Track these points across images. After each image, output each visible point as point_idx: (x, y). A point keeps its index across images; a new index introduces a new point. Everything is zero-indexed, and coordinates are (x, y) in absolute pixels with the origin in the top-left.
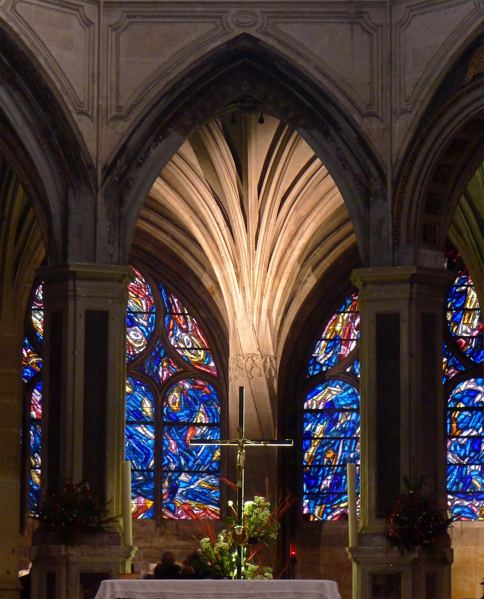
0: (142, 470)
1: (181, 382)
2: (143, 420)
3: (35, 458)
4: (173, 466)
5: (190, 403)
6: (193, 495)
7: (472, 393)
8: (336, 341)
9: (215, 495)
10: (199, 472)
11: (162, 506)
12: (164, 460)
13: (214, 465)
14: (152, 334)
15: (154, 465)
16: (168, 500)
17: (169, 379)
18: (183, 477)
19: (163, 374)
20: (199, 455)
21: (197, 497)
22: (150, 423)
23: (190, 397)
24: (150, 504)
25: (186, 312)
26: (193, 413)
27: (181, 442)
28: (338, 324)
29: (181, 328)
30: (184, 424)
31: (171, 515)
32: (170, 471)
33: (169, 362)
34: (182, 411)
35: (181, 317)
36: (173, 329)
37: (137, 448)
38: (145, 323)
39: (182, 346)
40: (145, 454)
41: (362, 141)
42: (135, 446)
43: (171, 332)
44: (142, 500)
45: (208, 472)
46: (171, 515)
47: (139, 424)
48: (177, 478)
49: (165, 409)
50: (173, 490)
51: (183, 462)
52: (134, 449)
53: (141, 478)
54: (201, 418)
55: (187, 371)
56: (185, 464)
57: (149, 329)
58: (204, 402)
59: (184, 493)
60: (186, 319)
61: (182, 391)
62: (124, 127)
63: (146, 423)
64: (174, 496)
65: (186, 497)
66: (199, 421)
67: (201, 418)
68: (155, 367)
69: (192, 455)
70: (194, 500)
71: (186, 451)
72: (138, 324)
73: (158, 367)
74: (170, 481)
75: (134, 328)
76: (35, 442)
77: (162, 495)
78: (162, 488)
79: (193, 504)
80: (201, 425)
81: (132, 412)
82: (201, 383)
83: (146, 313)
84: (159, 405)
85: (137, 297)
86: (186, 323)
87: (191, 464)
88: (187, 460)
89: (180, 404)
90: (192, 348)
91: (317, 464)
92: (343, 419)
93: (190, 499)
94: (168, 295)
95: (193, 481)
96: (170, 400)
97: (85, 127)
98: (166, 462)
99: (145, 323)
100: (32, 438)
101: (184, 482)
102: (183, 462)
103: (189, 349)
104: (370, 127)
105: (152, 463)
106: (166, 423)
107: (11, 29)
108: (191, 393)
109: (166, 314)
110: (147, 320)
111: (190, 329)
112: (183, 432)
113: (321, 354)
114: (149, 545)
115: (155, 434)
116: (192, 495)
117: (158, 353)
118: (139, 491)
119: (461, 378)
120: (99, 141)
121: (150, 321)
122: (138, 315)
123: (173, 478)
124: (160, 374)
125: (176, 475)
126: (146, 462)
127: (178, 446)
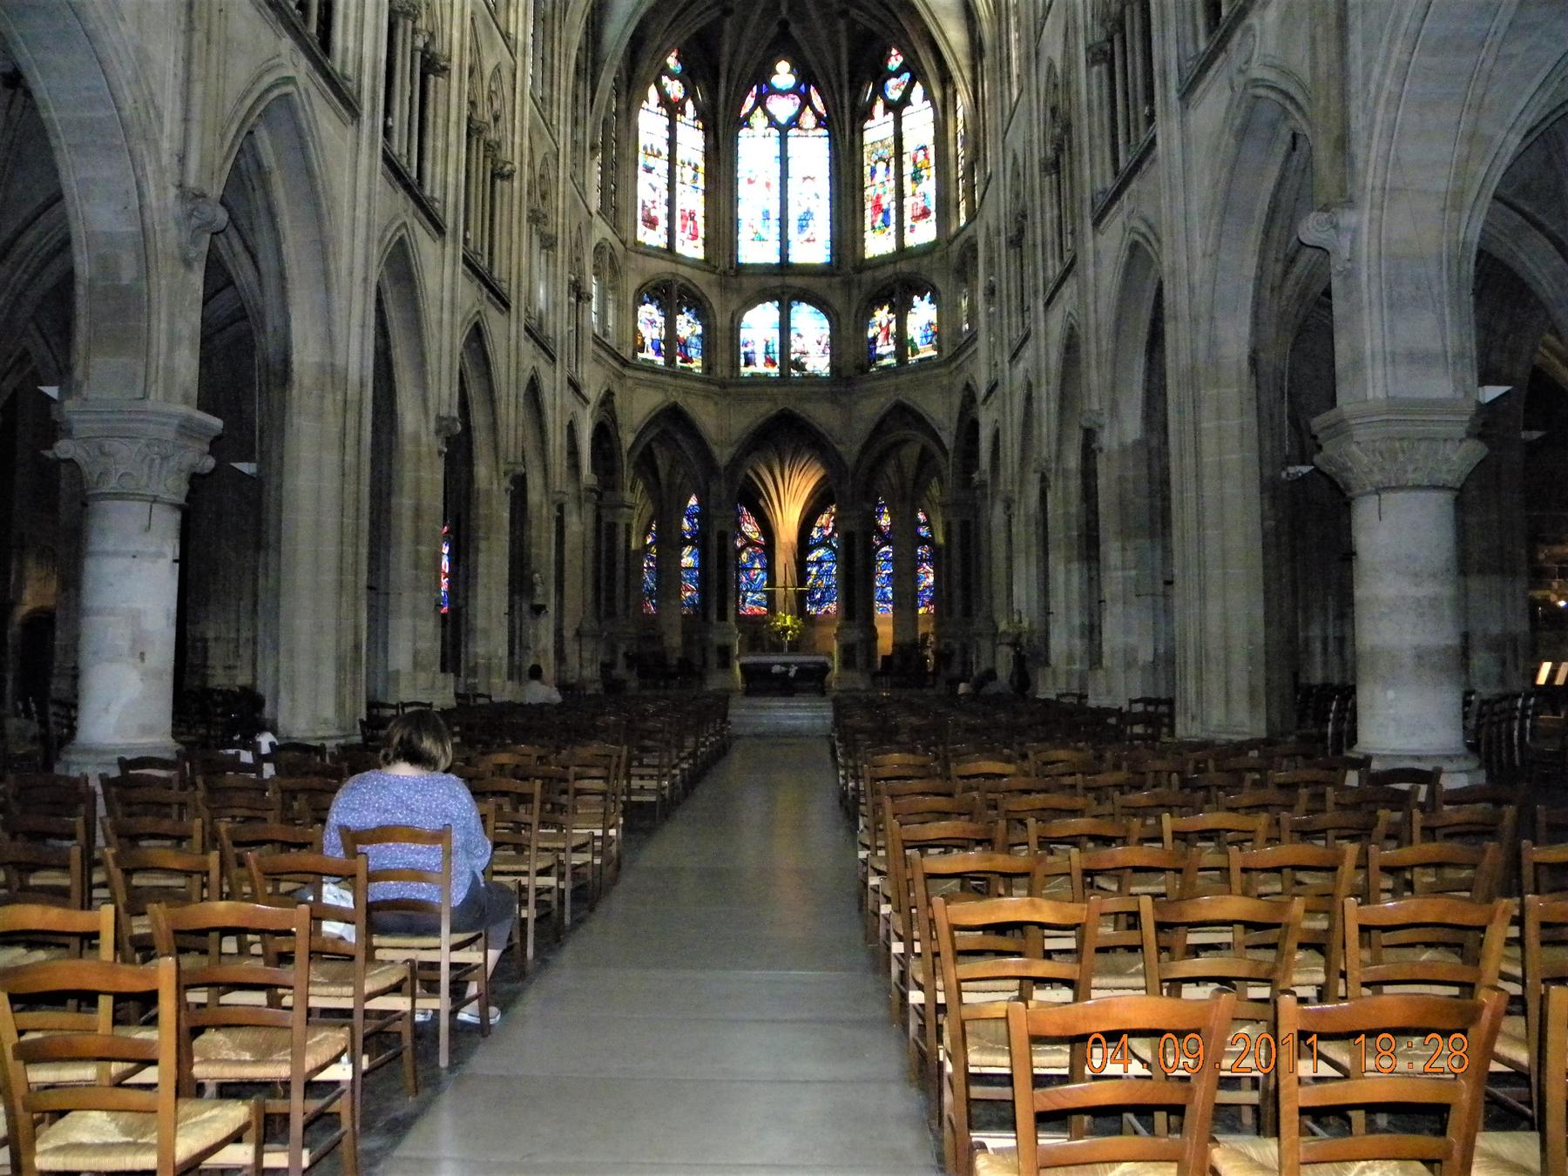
6: (754, 602)
7: (887, 553)
8: (822, 528)
28: (823, 519)
41: (839, 457)
50: (744, 600)
55: (750, 543)
62: (732, 450)
67: (757, 565)
71: (751, 581)
91: (814, 589)
92: (825, 566)
97: (716, 450)
104: (840, 448)
113: (815, 534)
119: (882, 546)
120: (722, 456)
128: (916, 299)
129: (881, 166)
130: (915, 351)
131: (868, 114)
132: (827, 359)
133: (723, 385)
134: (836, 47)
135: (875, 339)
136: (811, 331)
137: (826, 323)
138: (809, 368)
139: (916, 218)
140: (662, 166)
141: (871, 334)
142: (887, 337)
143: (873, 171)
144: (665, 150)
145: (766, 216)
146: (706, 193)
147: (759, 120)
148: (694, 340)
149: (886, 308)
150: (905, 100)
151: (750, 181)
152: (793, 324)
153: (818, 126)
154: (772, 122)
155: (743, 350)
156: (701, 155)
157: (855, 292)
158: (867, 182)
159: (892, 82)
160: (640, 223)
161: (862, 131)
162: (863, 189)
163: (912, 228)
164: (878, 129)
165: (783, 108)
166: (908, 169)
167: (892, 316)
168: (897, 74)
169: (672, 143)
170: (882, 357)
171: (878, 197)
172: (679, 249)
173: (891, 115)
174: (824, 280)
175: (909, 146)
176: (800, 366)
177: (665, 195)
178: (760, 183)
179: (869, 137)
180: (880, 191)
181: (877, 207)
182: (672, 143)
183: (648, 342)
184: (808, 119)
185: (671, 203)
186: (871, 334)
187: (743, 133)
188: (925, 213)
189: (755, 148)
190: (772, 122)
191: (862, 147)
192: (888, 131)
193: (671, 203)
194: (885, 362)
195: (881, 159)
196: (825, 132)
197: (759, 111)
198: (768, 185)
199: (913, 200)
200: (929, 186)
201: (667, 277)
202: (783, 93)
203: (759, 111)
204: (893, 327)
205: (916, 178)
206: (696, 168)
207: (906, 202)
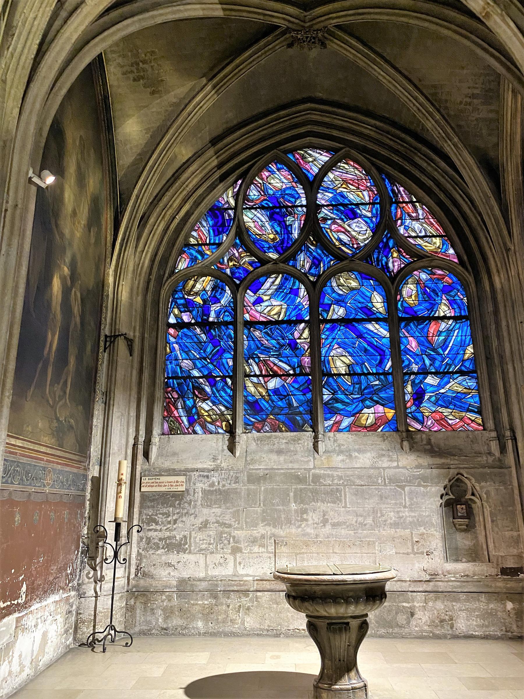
0: (378, 374)
1: (415, 272)
2: (374, 316)
3: (249, 365)
4: (415, 368)
5: (429, 296)
6: (444, 401)
9: (473, 400)
10: (448, 373)
11: (406, 416)
12: (403, 361)
13: (467, 364)
14: (378, 225)
15: (392, 366)
16: (414, 408)
17: (400, 270)
18: (430, 380)
19: (395, 264)
20: (446, 352)
21: (450, 403)
22: (384, 320)
23: (429, 288)
24: (390, 413)
25: (415, 200)
26: (433, 306)
27: (422, 339)
29: (410, 216)
30: (423, 319)
31: (419, 427)
32: (414, 373)
33: (399, 252)
34: (419, 304)
35: (410, 205)
36: (401, 218)
37: (369, 348)
38: (369, 215)
39: (413, 234)
40: (380, 355)
42: (366, 346)
43: (399, 221)
44: (380, 408)
45: (461, 373)
46: (419, 427)
47: (370, 321)
48: (421, 382)
49: (400, 303)
51: (427, 362)
52: (366, 350)
53: (377, 382)
54: (444, 310)
56: (431, 365)
57: (374, 220)
58: (447, 290)
59: (433, 399)
60: (415, 207)
61: (418, 282)
63: (377, 320)
64: (421, 403)
65: (436, 403)
66: (442, 314)
67: (444, 310)
68: (384, 258)
69: (439, 354)
70: (447, 407)
72: (361, 216)
73: (387, 257)
74: (413, 384)
75: (356, 220)
76: (249, 346)
77: (405, 402)
78: (404, 394)
79: (446, 412)
80: (444, 318)
81: (361, 308)
82: (440, 272)
83: (369, 204)
84: (391, 299)
85: (358, 188)
86: (416, 211)
87: (437, 364)
88: (433, 360)
89: (417, 296)
90: (426, 236)
93: (442, 406)
94: (392, 184)
95: (442, 384)
96: (404, 293)
98: (406, 363)
99: (369, 215)
100: (246, 342)
101: (432, 386)
102: (427, 362)
103: (422, 237)
105: (390, 364)
106: (402, 319)
108: (429, 284)
109: (392, 203)
110: (371, 211)
111: (421, 217)
112: (424, 328)
114: (395, 464)
115: (390, 331)
116: (444, 402)
117: (386, 245)
118: (375, 398)
121: (374, 211)
122: (361, 207)
123: (417, 381)
124: (390, 265)
125: (421, 377)
126: (381, 363)
127: (420, 343)
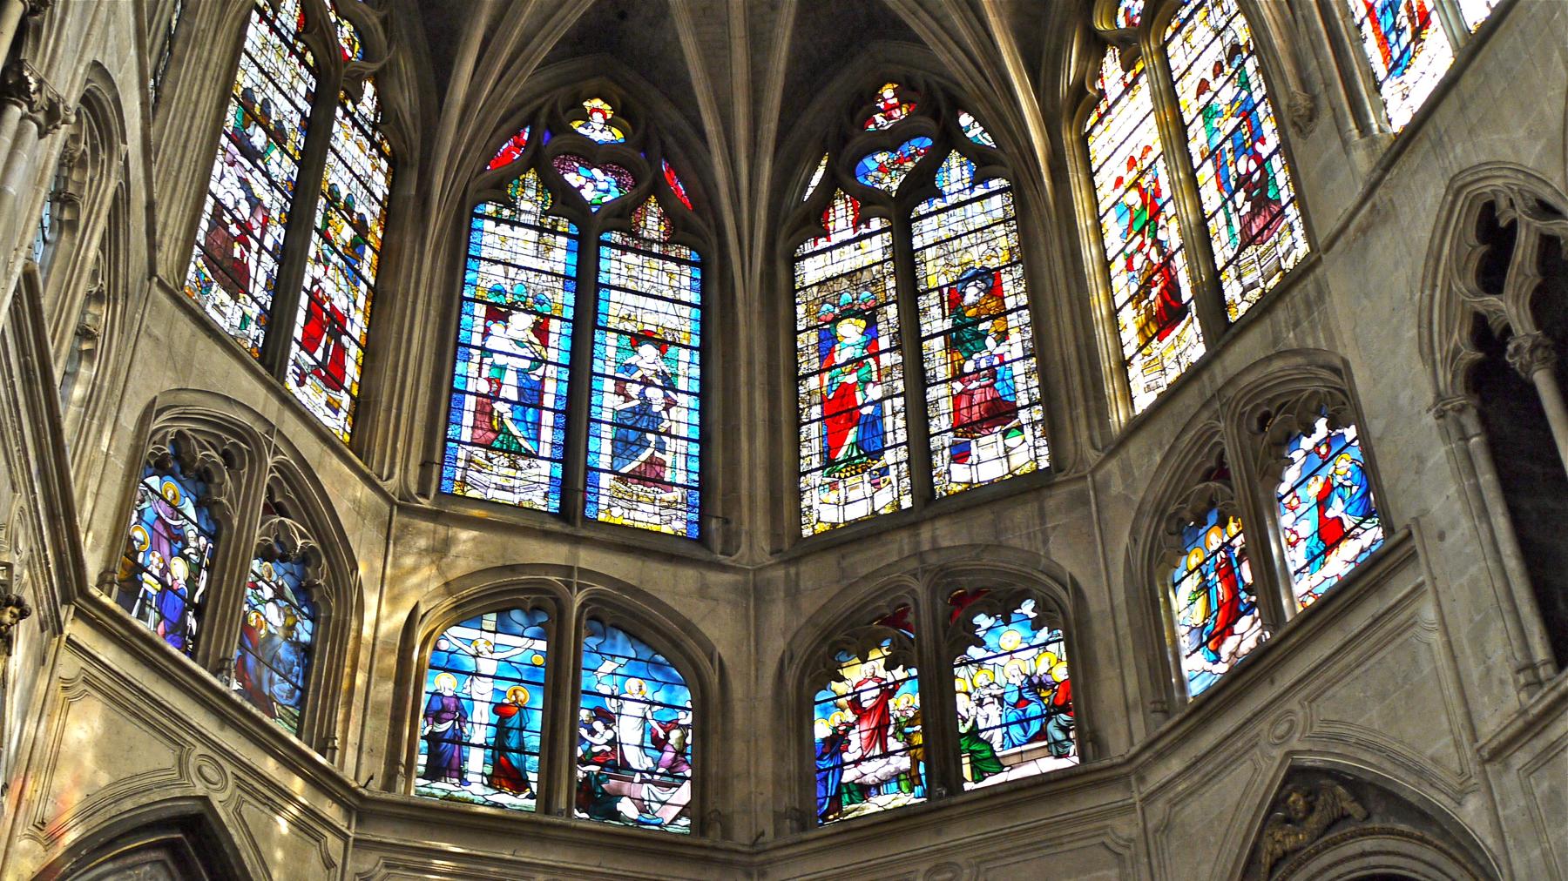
107: (230, 837)
128: (982, 620)
129: (851, 332)
130: (987, 762)
131: (815, 222)
132: (683, 794)
133: (359, 807)
134: (758, 43)
135: (837, 741)
136: (632, 706)
137: (684, 697)
138: (627, 808)
139: (967, 429)
140: (283, 167)
141: (822, 730)
142: (879, 734)
143: (828, 342)
144: (296, 139)
145: (531, 396)
146: (375, 295)
147: (530, 202)
148: (284, 652)
149: (877, 658)
150: (922, 185)
151: (497, 313)
152: (587, 681)
153: (672, 238)
154: (565, 201)
155: (424, 728)
156: (377, 208)
157: (778, 614)
158: (809, 362)
159: (882, 157)
160: (196, 250)
161: (793, 261)
162: (797, 379)
163: (960, 455)
164: (844, 253)
165: (596, 186)
166: (935, 321)
167: (899, 673)
168: (892, 140)
169: (317, 131)
170: (864, 791)
171: (846, 391)
172: (291, 383)
173: (876, 224)
174: (688, 576)
175: (934, 272)
176: (599, 801)
177: (276, 234)
178: (521, 323)
179: (812, 271)
180: (851, 379)
181: (841, 410)
182: (317, 131)
183: (150, 585)
184: (653, 225)
185: (290, 258)
186: (822, 730)
187: (490, 209)
188: (1000, 413)
189: (515, 251)
190: (565, 201)
191: (793, 293)
192: (876, 249)
193: (290, 258)
194: (874, 805)
195: (849, 312)
196: (695, 257)
197: (531, 176)
198: (541, 331)
199: (958, 386)
200: (1012, 348)
201: (245, 419)
202: (591, 155)
203: (531, 176)
204: (906, 701)
205: (962, 338)
206: (360, 227)
207: (933, 393)
